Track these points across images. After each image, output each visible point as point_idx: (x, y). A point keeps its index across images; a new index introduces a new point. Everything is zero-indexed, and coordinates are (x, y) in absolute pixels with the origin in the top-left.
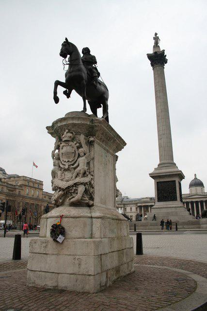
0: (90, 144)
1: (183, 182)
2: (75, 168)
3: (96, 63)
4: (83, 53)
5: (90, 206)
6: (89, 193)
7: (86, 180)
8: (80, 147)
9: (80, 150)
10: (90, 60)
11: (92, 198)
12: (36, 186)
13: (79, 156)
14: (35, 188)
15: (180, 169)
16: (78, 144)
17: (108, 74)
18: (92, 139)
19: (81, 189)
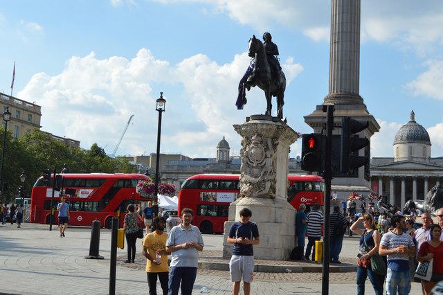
0: (275, 146)
1: (375, 140)
2: (262, 167)
3: (278, 54)
4: (264, 39)
5: (272, 198)
6: (273, 189)
7: (271, 178)
8: (267, 149)
9: (268, 153)
10: (273, 50)
11: (274, 192)
12: (24, 116)
13: (266, 157)
14: (22, 121)
15: (371, 112)
16: (265, 147)
17: (289, 66)
18: (276, 142)
19: (268, 185)
